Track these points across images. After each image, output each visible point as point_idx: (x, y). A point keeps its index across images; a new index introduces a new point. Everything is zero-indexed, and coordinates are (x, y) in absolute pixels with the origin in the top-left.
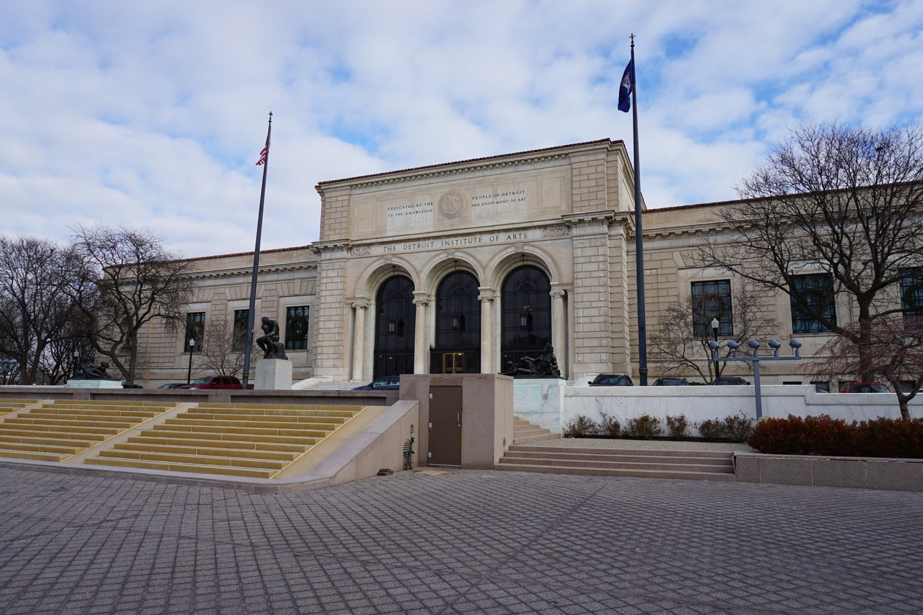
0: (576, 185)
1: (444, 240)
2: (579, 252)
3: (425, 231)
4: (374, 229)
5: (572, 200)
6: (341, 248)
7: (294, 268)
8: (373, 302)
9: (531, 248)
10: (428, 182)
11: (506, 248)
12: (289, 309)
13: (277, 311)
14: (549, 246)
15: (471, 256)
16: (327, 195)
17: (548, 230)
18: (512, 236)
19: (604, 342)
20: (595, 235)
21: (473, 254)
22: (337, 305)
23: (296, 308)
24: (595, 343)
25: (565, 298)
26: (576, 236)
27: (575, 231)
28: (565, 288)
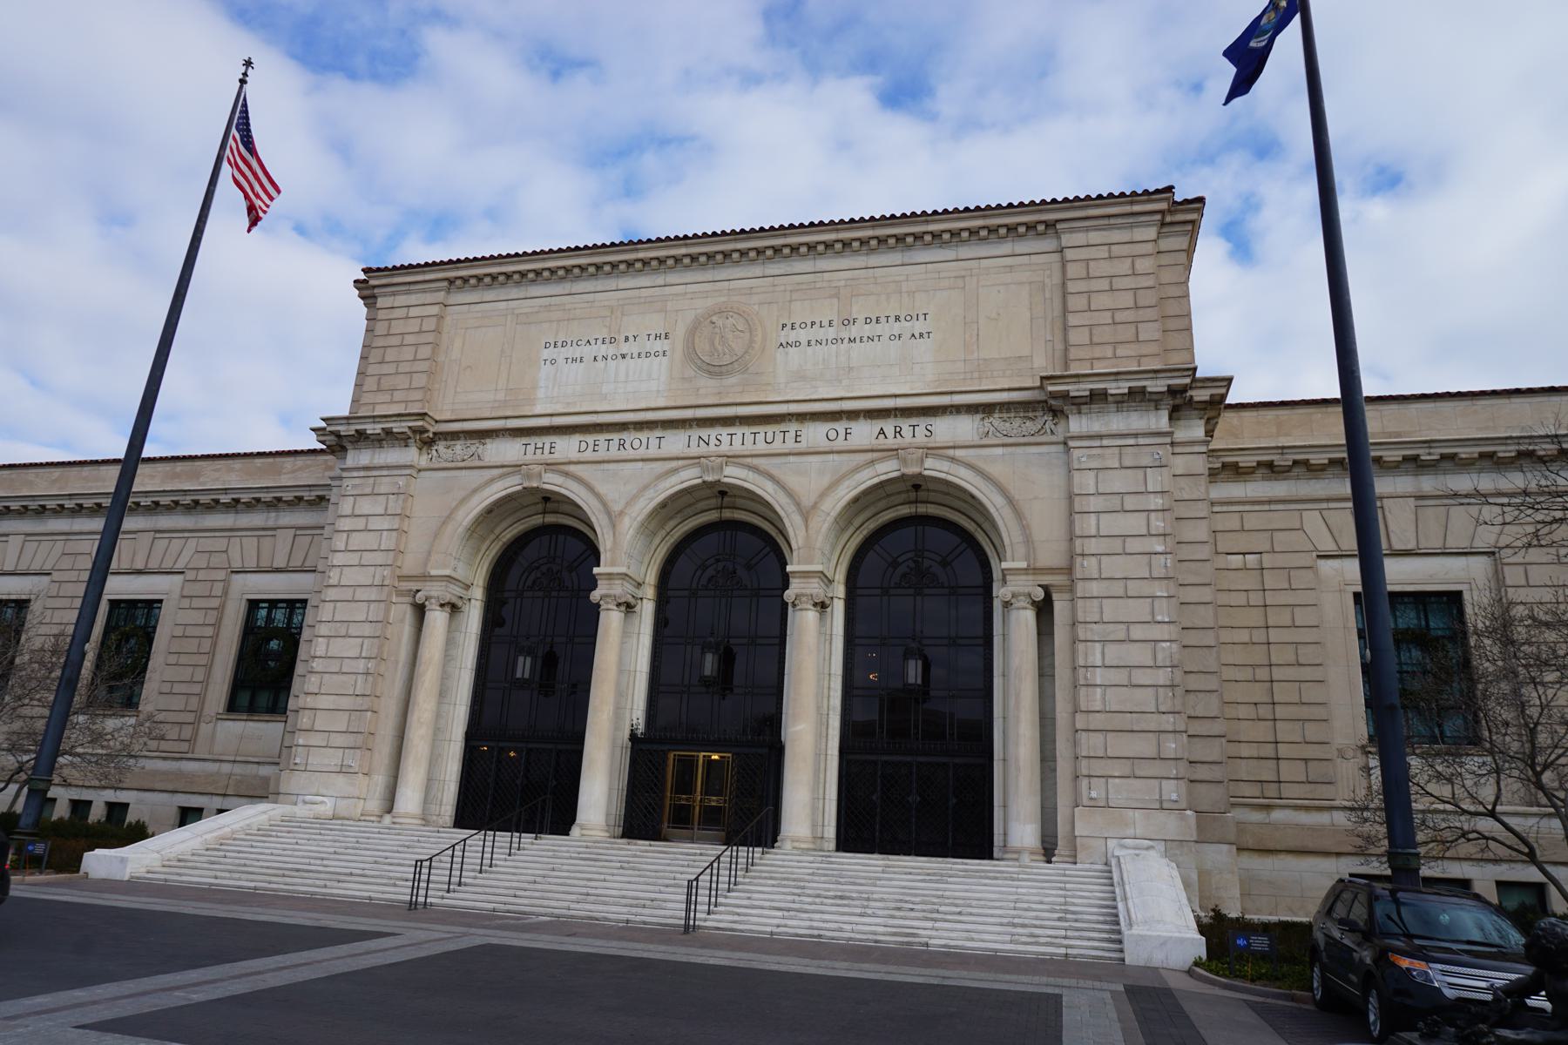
0: (1075, 303)
1: (696, 433)
2: (1085, 482)
3: (643, 405)
4: (501, 396)
5: (1066, 340)
6: (402, 440)
7: (279, 499)
8: (478, 593)
9: (944, 466)
10: (660, 280)
11: (872, 462)
12: (253, 605)
13: (221, 610)
14: (998, 462)
15: (771, 477)
16: (381, 302)
17: (996, 420)
18: (890, 430)
19: (1171, 746)
20: (1136, 435)
21: (775, 472)
22: (373, 594)
23: (273, 604)
24: (1144, 746)
25: (1044, 610)
26: (1080, 438)
27: (1077, 424)
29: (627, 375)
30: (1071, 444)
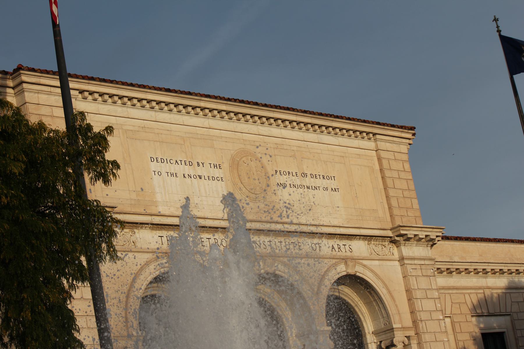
0: (389, 182)
20: (424, 259)
28: (408, 333)
29: (206, 192)
30: (406, 262)
